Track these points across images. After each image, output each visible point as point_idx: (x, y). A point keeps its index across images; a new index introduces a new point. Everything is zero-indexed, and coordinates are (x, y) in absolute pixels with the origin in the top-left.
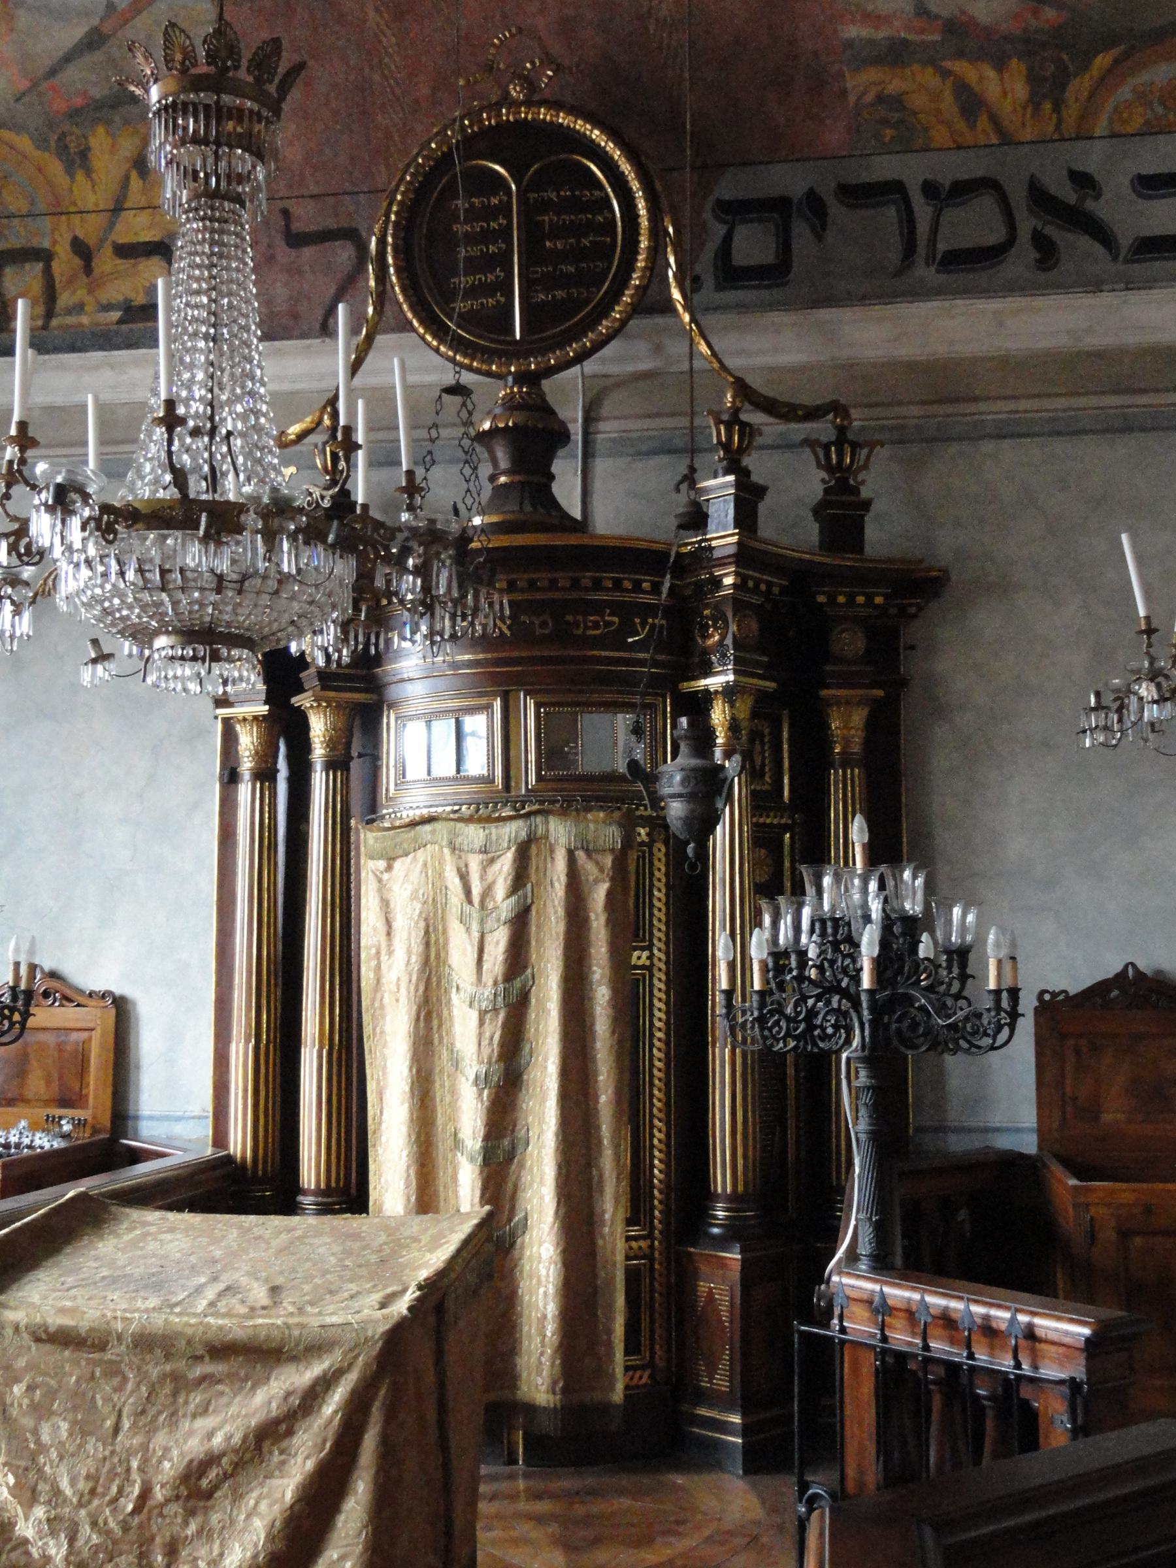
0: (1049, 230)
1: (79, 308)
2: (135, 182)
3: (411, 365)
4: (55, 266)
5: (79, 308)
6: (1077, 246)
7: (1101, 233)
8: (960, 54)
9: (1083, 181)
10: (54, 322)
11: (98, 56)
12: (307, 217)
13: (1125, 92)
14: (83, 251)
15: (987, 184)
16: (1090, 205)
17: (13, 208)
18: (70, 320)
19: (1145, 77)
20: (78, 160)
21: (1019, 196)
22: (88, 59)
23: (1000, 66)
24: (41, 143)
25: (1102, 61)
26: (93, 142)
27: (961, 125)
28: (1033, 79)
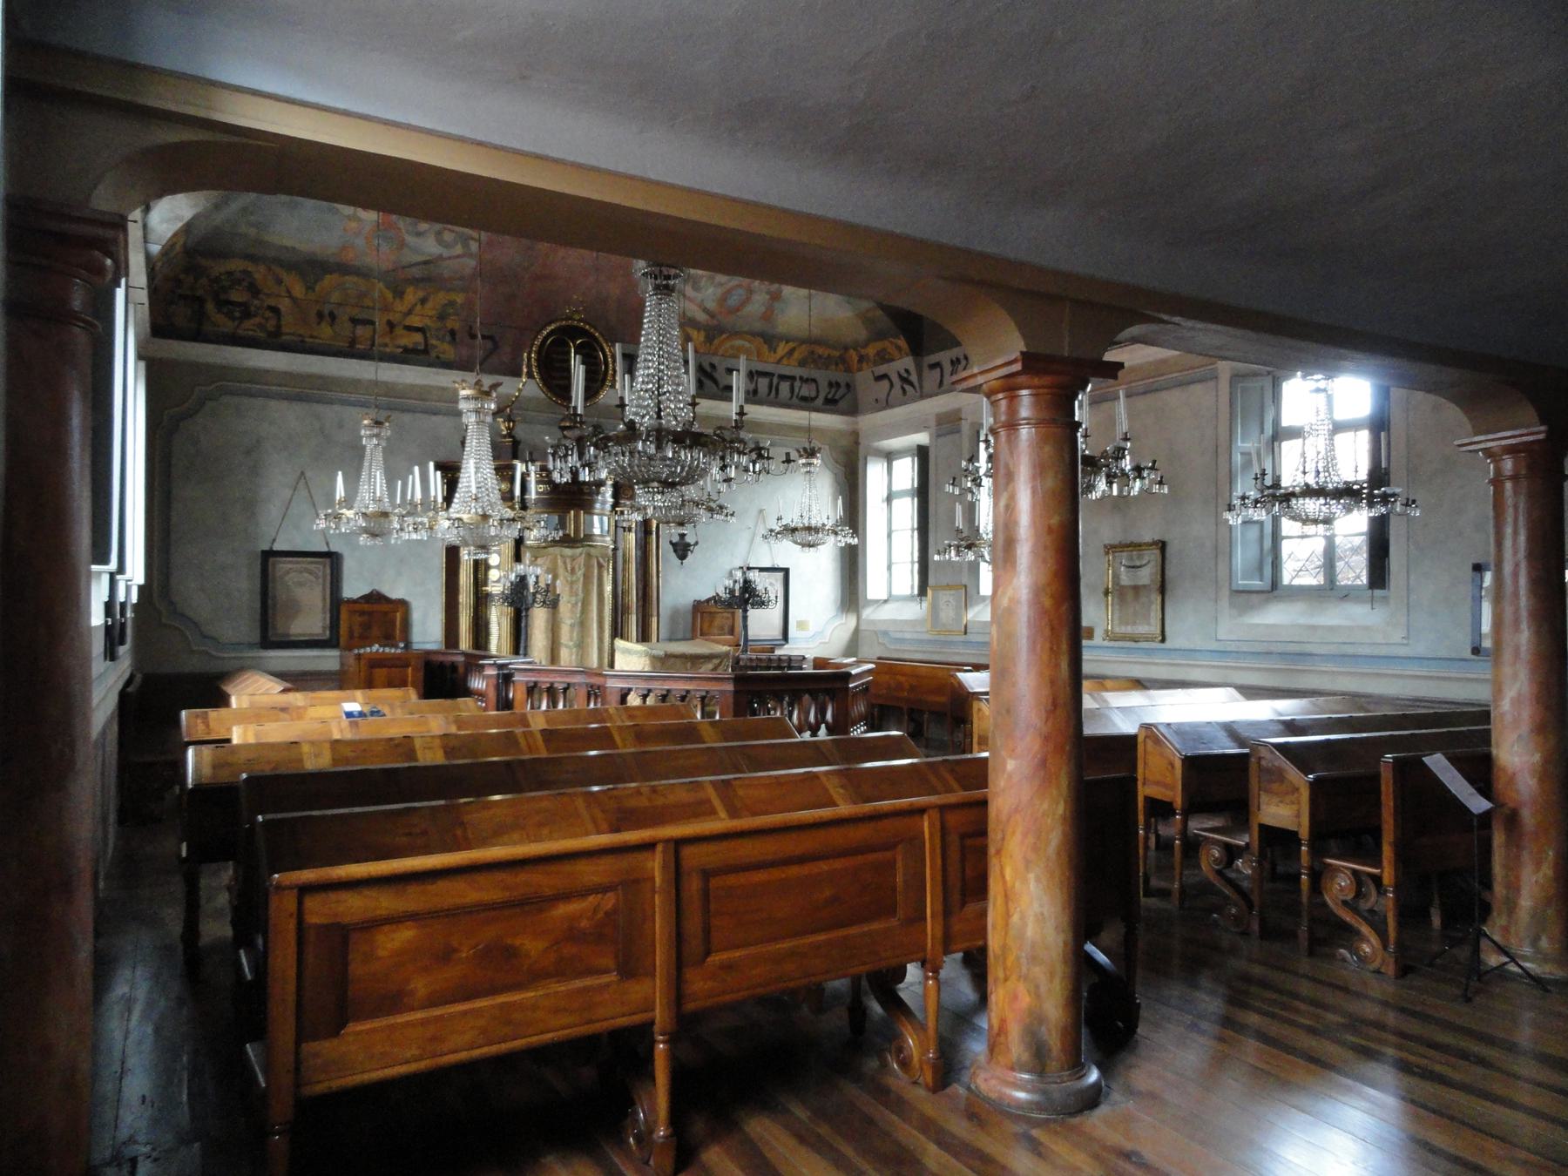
2: (419, 307)
7: (715, 382)
9: (713, 366)
13: (728, 345)
20: (399, 294)
23: (699, 330)
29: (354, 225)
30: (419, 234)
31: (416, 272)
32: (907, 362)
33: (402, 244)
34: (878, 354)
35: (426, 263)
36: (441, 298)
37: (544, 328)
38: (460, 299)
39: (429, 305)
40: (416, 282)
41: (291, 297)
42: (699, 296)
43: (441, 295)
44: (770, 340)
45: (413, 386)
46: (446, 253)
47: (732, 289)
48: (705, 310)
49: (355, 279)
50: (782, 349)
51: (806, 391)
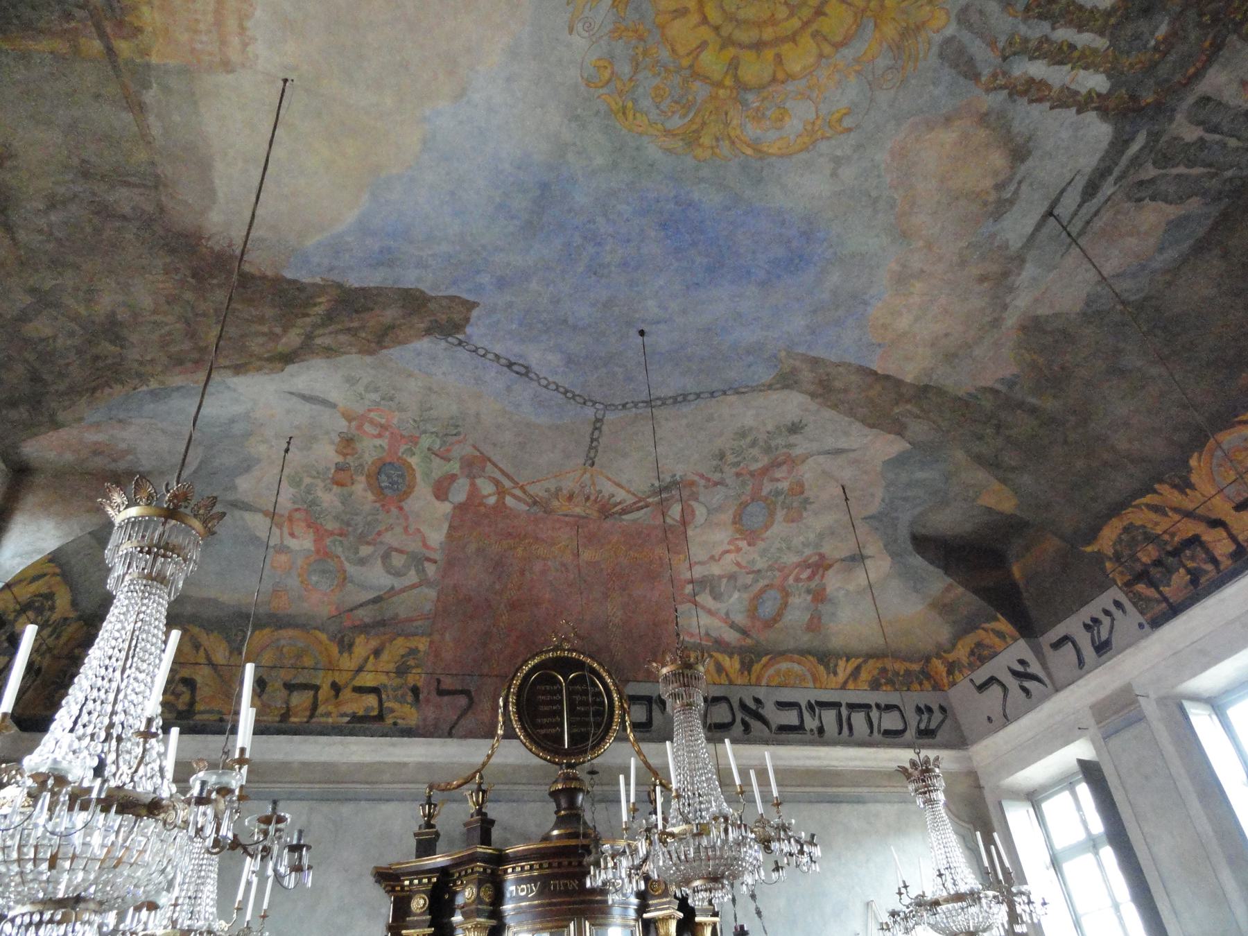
0: (747, 719)
1: (328, 714)
3: (514, 754)
4: (320, 692)
5: (328, 714)
6: (755, 725)
8: (718, 651)
9: (757, 701)
10: (314, 720)
11: (376, 607)
12: (448, 683)
13: (771, 671)
14: (336, 688)
15: (725, 699)
16: (760, 710)
17: (306, 665)
18: (323, 720)
19: (776, 667)
20: (346, 646)
21: (736, 705)
22: (371, 606)
23: (731, 658)
24: (332, 638)
25: (765, 660)
26: (358, 641)
27: (716, 675)
28: (742, 663)
29: (283, 558)
30: (362, 562)
31: (365, 615)
32: (1020, 649)
33: (345, 579)
34: (972, 653)
35: (376, 601)
36: (399, 646)
37: (525, 662)
38: (422, 644)
39: (385, 656)
40: (364, 628)
41: (210, 663)
42: (721, 607)
43: (400, 641)
44: (826, 658)
45: (361, 766)
46: (398, 583)
47: (763, 591)
48: (733, 626)
49: (291, 632)
50: (844, 669)
51: (891, 721)
